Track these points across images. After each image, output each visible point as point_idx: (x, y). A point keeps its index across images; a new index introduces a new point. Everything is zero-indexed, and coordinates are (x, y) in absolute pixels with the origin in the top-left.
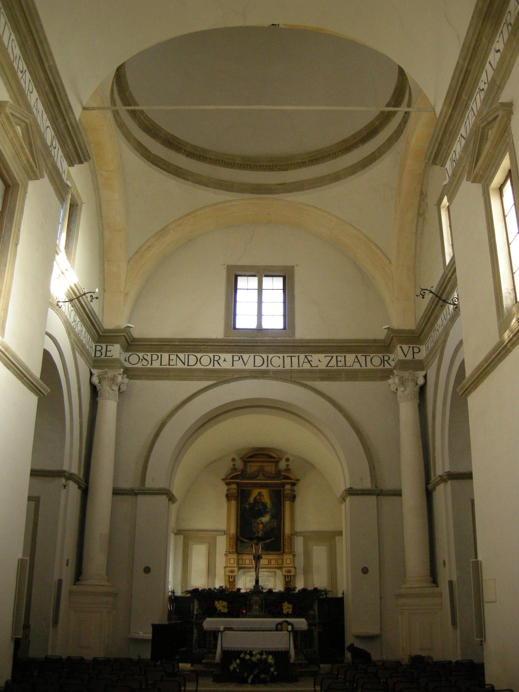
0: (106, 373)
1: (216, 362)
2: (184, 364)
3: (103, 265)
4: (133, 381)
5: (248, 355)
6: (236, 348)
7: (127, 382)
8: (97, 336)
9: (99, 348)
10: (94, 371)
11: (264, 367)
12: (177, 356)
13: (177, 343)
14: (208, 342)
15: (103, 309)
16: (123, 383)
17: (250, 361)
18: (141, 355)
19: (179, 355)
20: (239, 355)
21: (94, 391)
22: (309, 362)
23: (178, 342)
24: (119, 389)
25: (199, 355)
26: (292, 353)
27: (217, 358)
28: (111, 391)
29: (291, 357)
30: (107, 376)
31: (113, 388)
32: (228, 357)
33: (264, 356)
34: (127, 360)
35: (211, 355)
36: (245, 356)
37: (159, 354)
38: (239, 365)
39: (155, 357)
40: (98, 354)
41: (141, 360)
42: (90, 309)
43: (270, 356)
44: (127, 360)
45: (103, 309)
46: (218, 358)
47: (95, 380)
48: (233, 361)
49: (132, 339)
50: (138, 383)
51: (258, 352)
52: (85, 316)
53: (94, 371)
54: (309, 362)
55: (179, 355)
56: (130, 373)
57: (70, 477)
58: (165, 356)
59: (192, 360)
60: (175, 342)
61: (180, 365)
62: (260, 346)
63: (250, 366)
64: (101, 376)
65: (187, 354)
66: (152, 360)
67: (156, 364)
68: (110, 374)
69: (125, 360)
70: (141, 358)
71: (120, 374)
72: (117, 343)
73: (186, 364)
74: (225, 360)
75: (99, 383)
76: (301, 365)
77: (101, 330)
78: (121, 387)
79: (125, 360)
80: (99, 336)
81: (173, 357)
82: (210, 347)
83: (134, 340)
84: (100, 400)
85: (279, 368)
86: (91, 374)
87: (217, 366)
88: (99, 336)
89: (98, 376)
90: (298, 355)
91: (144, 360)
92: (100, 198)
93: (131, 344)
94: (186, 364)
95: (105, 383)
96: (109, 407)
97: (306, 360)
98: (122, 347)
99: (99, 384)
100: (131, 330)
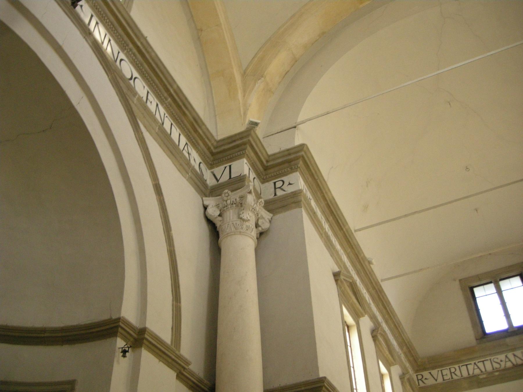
10: (210, 202)
21: (214, 230)
24: (257, 226)
28: (238, 222)
30: (229, 202)
64: (221, 206)
68: (235, 196)
71: (250, 192)
75: (220, 215)
78: (260, 223)
84: (225, 243)
86: (205, 208)
95: (231, 215)
98: (253, 166)
99: (220, 218)
100: (260, 132)
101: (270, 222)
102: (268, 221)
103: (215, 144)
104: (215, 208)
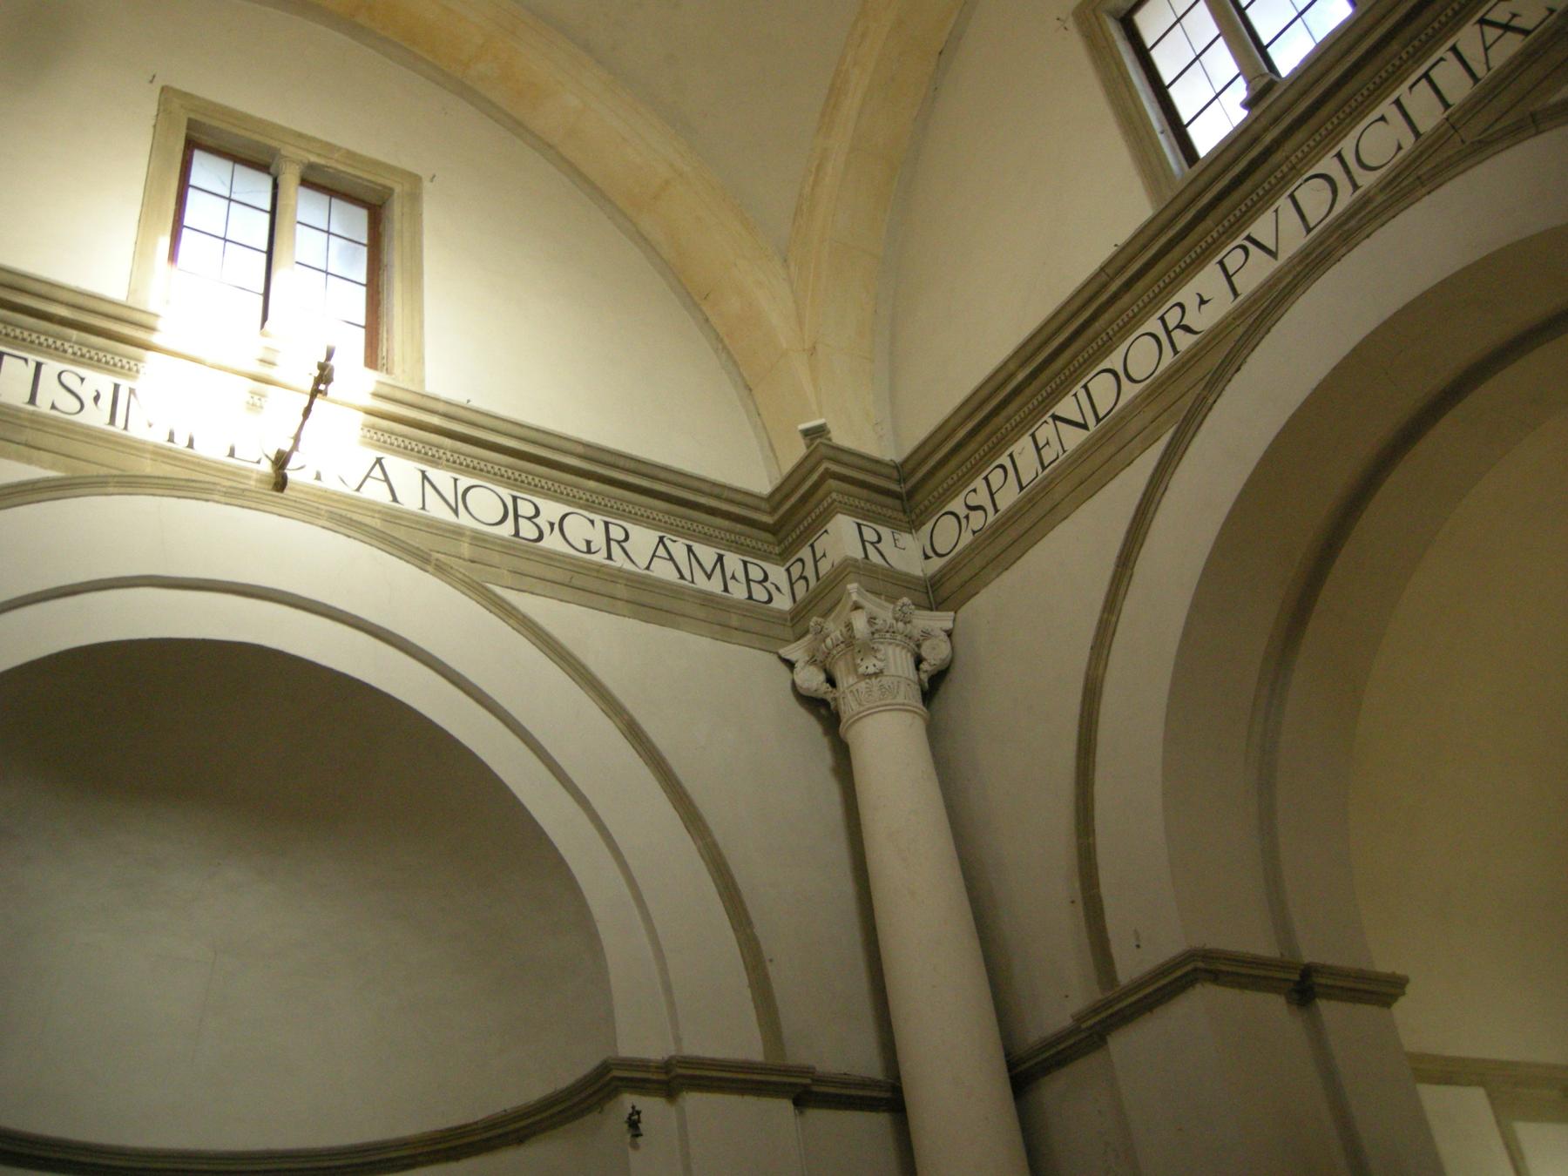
0: (821, 634)
1: (1178, 335)
2: (1085, 426)
3: (707, 320)
4: (964, 611)
5: (1269, 215)
6: (1209, 222)
7: (949, 625)
8: (769, 537)
9: (796, 570)
10: (795, 652)
11: (1346, 198)
12: (1055, 418)
13: (1020, 376)
14: (1105, 286)
15: (771, 445)
16: (927, 635)
17: (1281, 228)
18: (957, 505)
19: (1059, 409)
20: (1239, 241)
22: (1506, 27)
23: (1022, 365)
25: (1114, 361)
26: (1419, 62)
27: (1173, 318)
28: (863, 685)
29: (1426, 76)
31: (861, 670)
32: (1208, 280)
33: (1328, 165)
34: (930, 553)
35: (1153, 325)
36: (1261, 228)
37: (1004, 460)
38: (1255, 272)
39: (996, 477)
40: (800, 588)
41: (964, 522)
42: (580, 450)
43: (1347, 146)
44: (930, 553)
45: (771, 445)
46: (1177, 310)
47: (811, 679)
48: (1229, 277)
49: (895, 474)
50: (983, 603)
51: (1295, 171)
52: (592, 484)
53: (795, 652)
54: (1506, 27)
55: (1059, 409)
56: (939, 592)
57: (675, 1078)
58: (1023, 448)
59: (1102, 387)
60: (1012, 375)
61: (1074, 438)
62: (1277, 144)
63: (1293, 240)
64: (820, 657)
65: (1078, 388)
66: (992, 495)
67: (1008, 497)
69: (927, 557)
70: (962, 512)
72: (827, 515)
73: (1091, 421)
74: (1203, 302)
76: (1480, 70)
77: (757, 509)
78: (924, 652)
79: (927, 557)
80: (772, 530)
81: (1046, 431)
82: (1126, 299)
83: (902, 470)
85: (1401, 154)
87: (1184, 341)
88: (772, 530)
89: (812, 661)
90: (1449, 44)
91: (972, 514)
92: (550, 146)
93: (904, 492)
94: (1091, 421)
96: (889, 741)
97: (1492, 33)
101: (949, 634)
102: (943, 636)
103: (764, 505)
104: (813, 670)
